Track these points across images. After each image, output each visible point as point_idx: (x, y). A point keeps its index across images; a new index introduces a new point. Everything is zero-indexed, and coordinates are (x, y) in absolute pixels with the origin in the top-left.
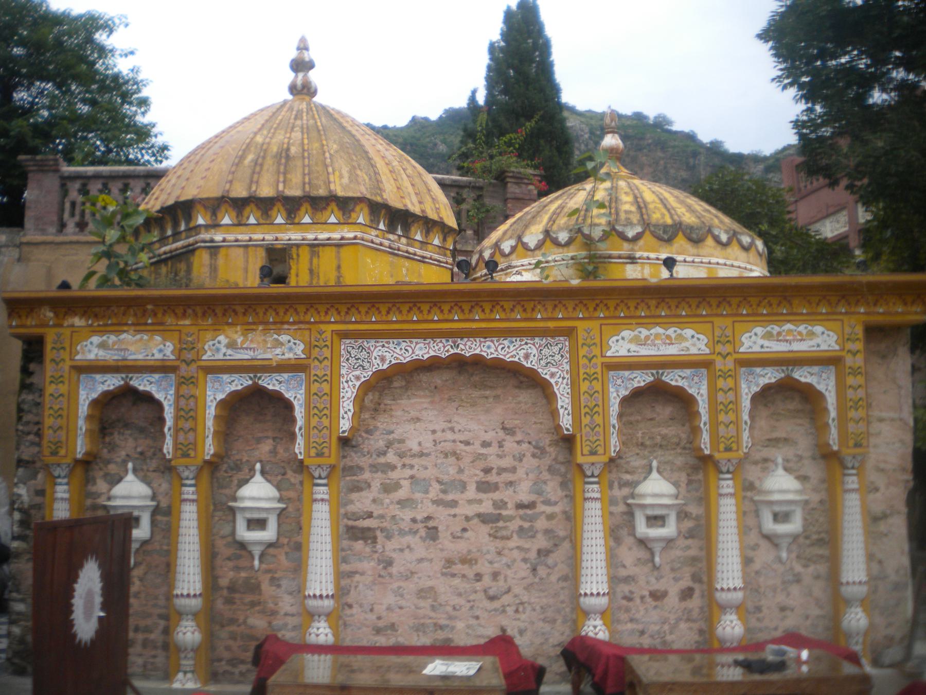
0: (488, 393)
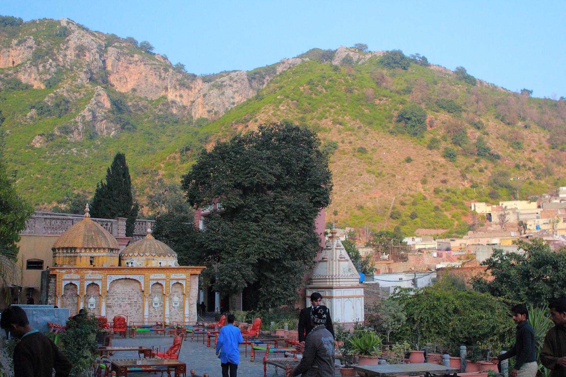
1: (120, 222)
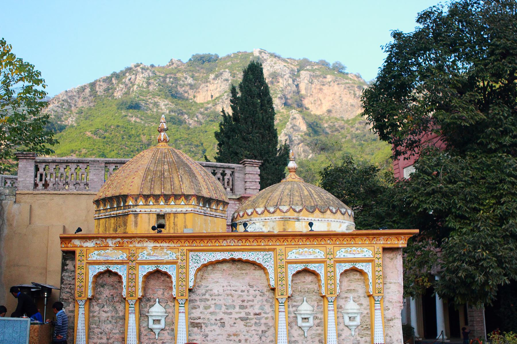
0: (243, 272)
1: (248, 169)
